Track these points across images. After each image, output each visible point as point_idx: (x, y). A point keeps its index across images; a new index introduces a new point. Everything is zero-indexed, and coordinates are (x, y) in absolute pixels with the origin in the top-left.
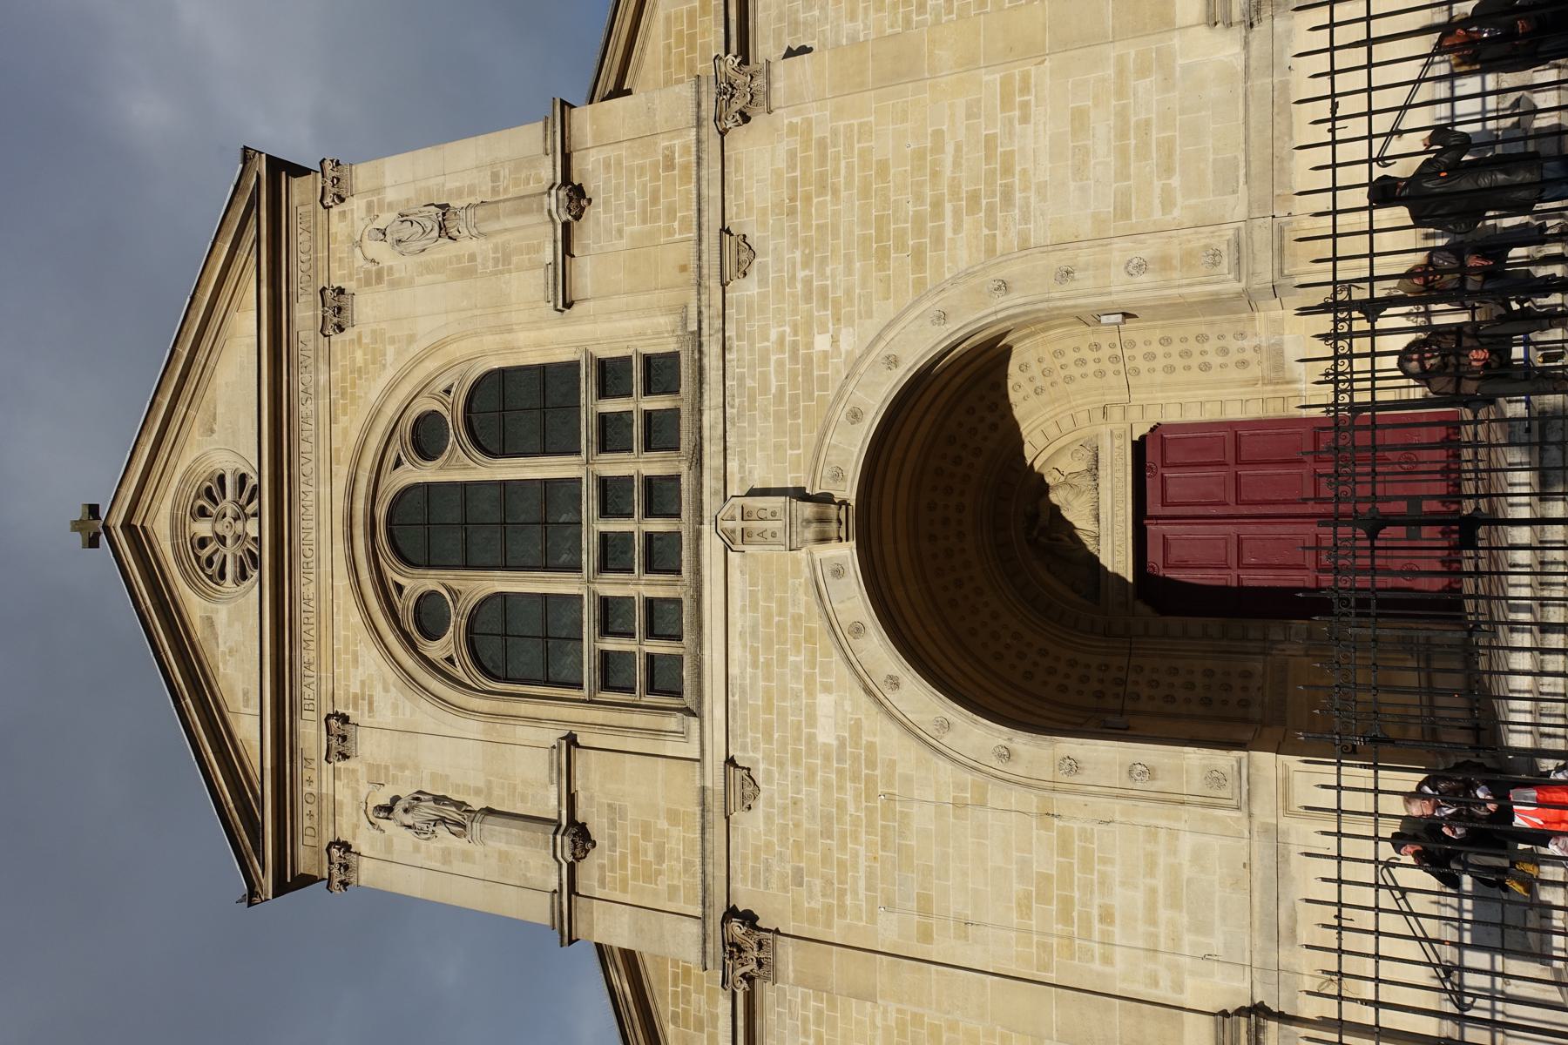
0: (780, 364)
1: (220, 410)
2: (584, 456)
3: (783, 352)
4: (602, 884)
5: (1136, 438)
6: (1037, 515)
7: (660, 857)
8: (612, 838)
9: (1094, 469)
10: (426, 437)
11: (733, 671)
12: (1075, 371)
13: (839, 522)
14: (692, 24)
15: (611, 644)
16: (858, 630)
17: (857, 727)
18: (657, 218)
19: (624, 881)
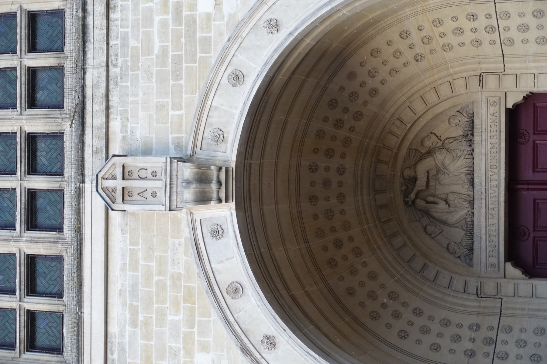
0: (164, 24)
3: (167, 13)
5: (510, 106)
6: (414, 180)
9: (469, 134)
11: (113, 329)
12: (454, 40)
13: (220, 183)
16: (236, 290)
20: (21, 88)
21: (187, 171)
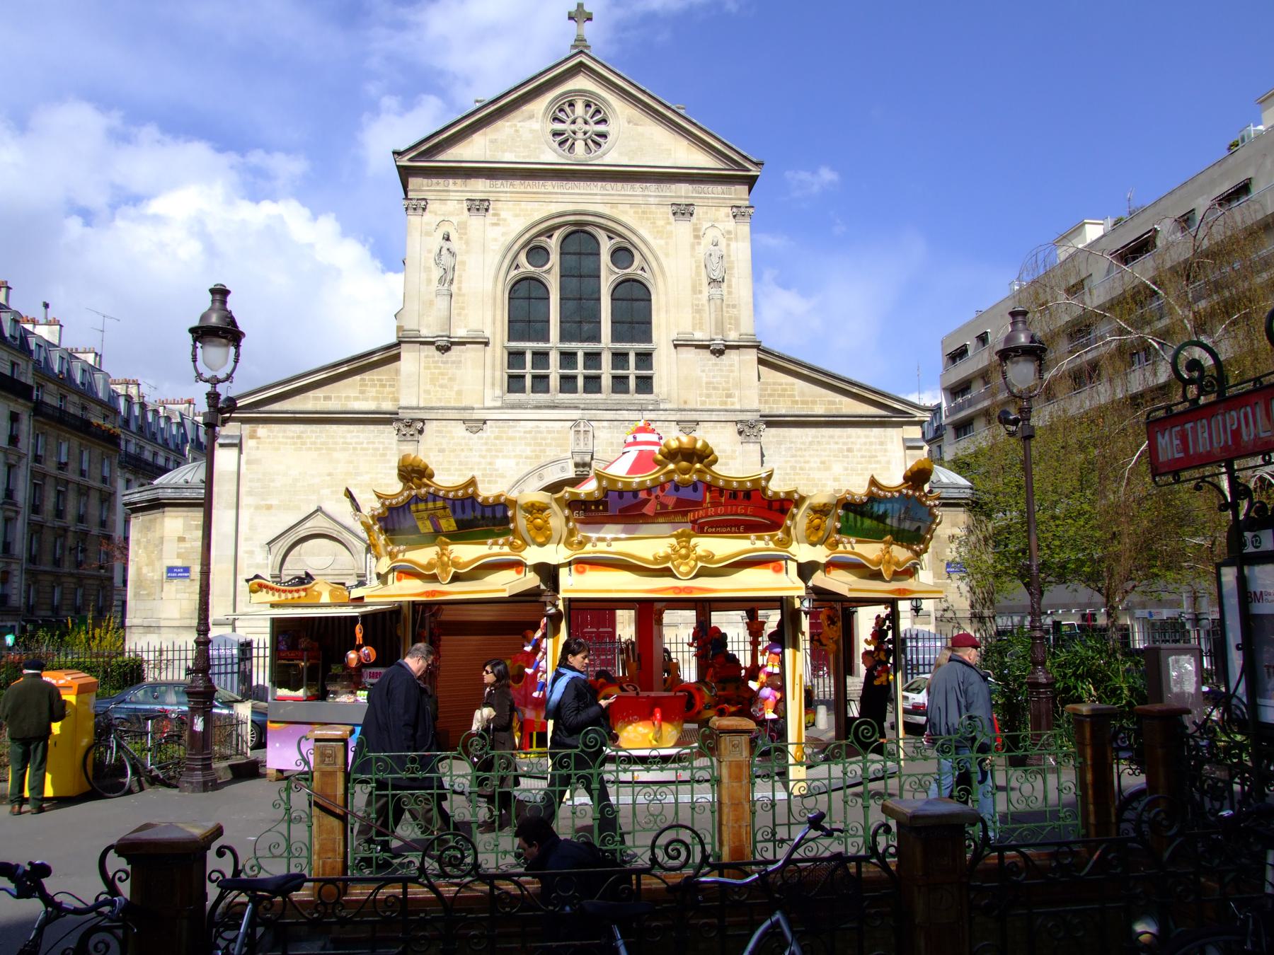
1: (640, 129)
2: (610, 345)
4: (427, 357)
7: (442, 386)
8: (446, 362)
10: (623, 254)
14: (790, 396)
15: (529, 357)
16: (541, 477)
17: (503, 476)
18: (707, 388)
19: (428, 368)
20: (620, 372)
21: (588, 459)
